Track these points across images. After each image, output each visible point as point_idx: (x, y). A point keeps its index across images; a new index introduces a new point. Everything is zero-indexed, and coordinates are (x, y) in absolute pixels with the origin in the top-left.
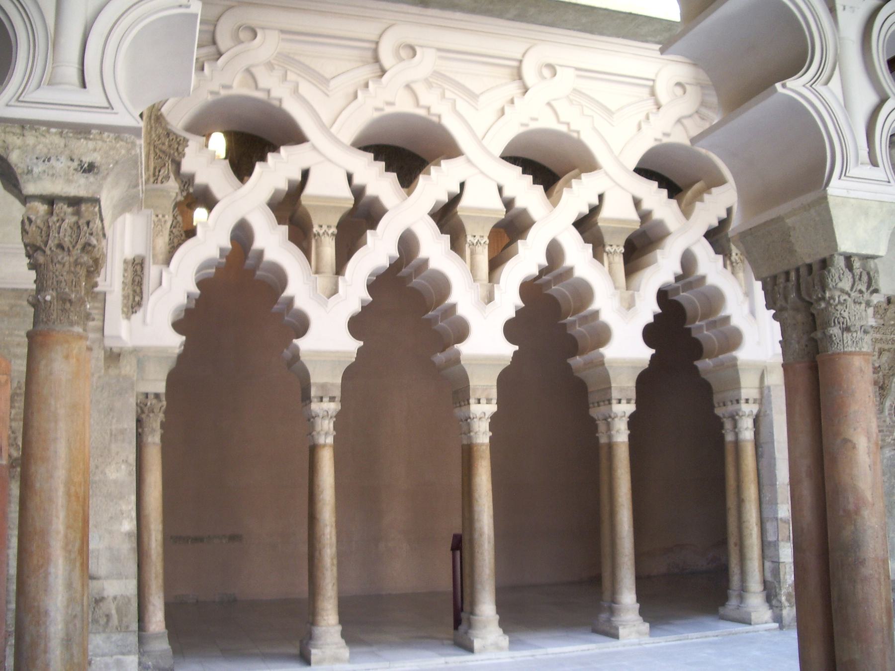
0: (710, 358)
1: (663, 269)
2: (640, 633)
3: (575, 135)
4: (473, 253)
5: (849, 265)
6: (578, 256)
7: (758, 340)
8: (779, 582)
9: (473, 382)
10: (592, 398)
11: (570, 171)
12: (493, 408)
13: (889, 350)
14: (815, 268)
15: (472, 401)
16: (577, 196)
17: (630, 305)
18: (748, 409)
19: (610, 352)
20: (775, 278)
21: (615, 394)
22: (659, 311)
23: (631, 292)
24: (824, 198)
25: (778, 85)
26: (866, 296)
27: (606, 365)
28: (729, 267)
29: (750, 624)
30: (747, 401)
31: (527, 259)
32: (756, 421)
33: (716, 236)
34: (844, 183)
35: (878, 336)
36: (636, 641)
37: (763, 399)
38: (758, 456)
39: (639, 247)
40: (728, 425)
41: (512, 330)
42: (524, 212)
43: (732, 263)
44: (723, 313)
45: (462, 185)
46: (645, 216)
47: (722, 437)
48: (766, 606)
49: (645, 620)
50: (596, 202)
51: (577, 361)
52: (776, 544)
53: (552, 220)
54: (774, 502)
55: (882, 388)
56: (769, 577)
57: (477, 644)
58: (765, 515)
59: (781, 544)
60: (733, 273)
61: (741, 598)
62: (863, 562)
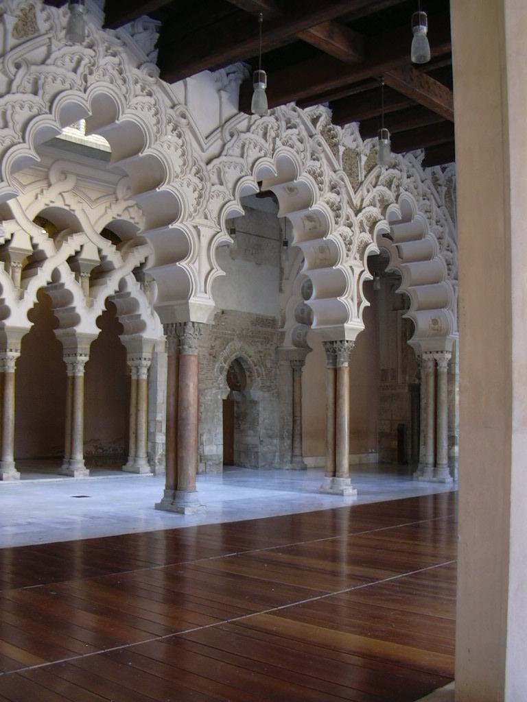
0: (128, 334)
1: (109, 287)
2: (85, 475)
3: (72, 212)
4: (13, 272)
5: (193, 326)
6: (67, 278)
7: (154, 331)
8: (155, 453)
9: (9, 341)
10: (66, 352)
11: (64, 229)
12: (18, 354)
13: (220, 338)
14: (183, 325)
15: (8, 350)
16: (71, 245)
17: (91, 305)
18: (146, 363)
19: (79, 329)
20: (168, 324)
21: (79, 351)
22: (105, 309)
23: (91, 299)
24: (187, 304)
25: (177, 263)
26: (198, 336)
27: (77, 336)
28: (143, 288)
29: (138, 473)
30: (145, 359)
31: (42, 278)
32: (148, 370)
33: (138, 272)
34: (194, 299)
35: (215, 330)
36: (83, 478)
37: (154, 359)
38: (148, 388)
39: (99, 273)
40: (134, 371)
41: (31, 315)
42: (42, 251)
43: (144, 286)
44: (137, 313)
45: (12, 235)
46: (103, 258)
47: (130, 377)
48: (147, 464)
49: (87, 468)
50: (79, 249)
51: (58, 332)
52: (154, 434)
53: (56, 260)
54: (155, 412)
55: (214, 357)
56: (150, 451)
57: (5, 476)
58: (150, 418)
59: (157, 433)
60: (144, 291)
61: (135, 461)
62: (188, 424)
